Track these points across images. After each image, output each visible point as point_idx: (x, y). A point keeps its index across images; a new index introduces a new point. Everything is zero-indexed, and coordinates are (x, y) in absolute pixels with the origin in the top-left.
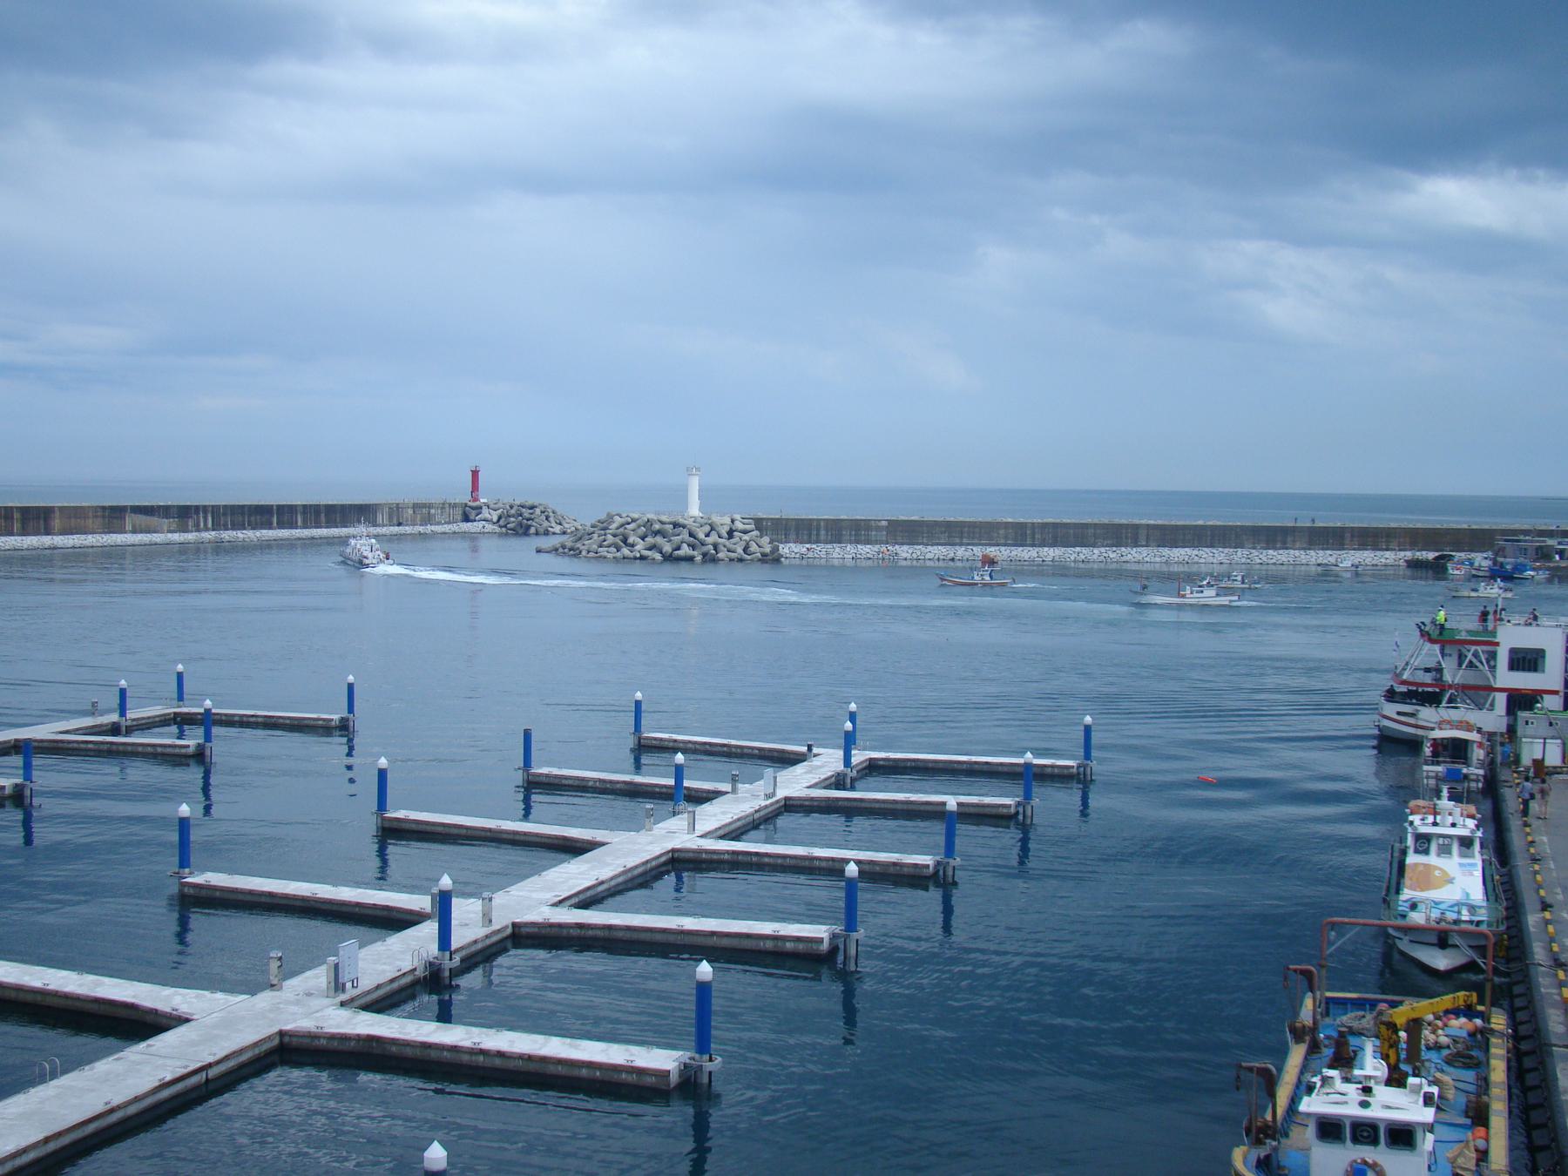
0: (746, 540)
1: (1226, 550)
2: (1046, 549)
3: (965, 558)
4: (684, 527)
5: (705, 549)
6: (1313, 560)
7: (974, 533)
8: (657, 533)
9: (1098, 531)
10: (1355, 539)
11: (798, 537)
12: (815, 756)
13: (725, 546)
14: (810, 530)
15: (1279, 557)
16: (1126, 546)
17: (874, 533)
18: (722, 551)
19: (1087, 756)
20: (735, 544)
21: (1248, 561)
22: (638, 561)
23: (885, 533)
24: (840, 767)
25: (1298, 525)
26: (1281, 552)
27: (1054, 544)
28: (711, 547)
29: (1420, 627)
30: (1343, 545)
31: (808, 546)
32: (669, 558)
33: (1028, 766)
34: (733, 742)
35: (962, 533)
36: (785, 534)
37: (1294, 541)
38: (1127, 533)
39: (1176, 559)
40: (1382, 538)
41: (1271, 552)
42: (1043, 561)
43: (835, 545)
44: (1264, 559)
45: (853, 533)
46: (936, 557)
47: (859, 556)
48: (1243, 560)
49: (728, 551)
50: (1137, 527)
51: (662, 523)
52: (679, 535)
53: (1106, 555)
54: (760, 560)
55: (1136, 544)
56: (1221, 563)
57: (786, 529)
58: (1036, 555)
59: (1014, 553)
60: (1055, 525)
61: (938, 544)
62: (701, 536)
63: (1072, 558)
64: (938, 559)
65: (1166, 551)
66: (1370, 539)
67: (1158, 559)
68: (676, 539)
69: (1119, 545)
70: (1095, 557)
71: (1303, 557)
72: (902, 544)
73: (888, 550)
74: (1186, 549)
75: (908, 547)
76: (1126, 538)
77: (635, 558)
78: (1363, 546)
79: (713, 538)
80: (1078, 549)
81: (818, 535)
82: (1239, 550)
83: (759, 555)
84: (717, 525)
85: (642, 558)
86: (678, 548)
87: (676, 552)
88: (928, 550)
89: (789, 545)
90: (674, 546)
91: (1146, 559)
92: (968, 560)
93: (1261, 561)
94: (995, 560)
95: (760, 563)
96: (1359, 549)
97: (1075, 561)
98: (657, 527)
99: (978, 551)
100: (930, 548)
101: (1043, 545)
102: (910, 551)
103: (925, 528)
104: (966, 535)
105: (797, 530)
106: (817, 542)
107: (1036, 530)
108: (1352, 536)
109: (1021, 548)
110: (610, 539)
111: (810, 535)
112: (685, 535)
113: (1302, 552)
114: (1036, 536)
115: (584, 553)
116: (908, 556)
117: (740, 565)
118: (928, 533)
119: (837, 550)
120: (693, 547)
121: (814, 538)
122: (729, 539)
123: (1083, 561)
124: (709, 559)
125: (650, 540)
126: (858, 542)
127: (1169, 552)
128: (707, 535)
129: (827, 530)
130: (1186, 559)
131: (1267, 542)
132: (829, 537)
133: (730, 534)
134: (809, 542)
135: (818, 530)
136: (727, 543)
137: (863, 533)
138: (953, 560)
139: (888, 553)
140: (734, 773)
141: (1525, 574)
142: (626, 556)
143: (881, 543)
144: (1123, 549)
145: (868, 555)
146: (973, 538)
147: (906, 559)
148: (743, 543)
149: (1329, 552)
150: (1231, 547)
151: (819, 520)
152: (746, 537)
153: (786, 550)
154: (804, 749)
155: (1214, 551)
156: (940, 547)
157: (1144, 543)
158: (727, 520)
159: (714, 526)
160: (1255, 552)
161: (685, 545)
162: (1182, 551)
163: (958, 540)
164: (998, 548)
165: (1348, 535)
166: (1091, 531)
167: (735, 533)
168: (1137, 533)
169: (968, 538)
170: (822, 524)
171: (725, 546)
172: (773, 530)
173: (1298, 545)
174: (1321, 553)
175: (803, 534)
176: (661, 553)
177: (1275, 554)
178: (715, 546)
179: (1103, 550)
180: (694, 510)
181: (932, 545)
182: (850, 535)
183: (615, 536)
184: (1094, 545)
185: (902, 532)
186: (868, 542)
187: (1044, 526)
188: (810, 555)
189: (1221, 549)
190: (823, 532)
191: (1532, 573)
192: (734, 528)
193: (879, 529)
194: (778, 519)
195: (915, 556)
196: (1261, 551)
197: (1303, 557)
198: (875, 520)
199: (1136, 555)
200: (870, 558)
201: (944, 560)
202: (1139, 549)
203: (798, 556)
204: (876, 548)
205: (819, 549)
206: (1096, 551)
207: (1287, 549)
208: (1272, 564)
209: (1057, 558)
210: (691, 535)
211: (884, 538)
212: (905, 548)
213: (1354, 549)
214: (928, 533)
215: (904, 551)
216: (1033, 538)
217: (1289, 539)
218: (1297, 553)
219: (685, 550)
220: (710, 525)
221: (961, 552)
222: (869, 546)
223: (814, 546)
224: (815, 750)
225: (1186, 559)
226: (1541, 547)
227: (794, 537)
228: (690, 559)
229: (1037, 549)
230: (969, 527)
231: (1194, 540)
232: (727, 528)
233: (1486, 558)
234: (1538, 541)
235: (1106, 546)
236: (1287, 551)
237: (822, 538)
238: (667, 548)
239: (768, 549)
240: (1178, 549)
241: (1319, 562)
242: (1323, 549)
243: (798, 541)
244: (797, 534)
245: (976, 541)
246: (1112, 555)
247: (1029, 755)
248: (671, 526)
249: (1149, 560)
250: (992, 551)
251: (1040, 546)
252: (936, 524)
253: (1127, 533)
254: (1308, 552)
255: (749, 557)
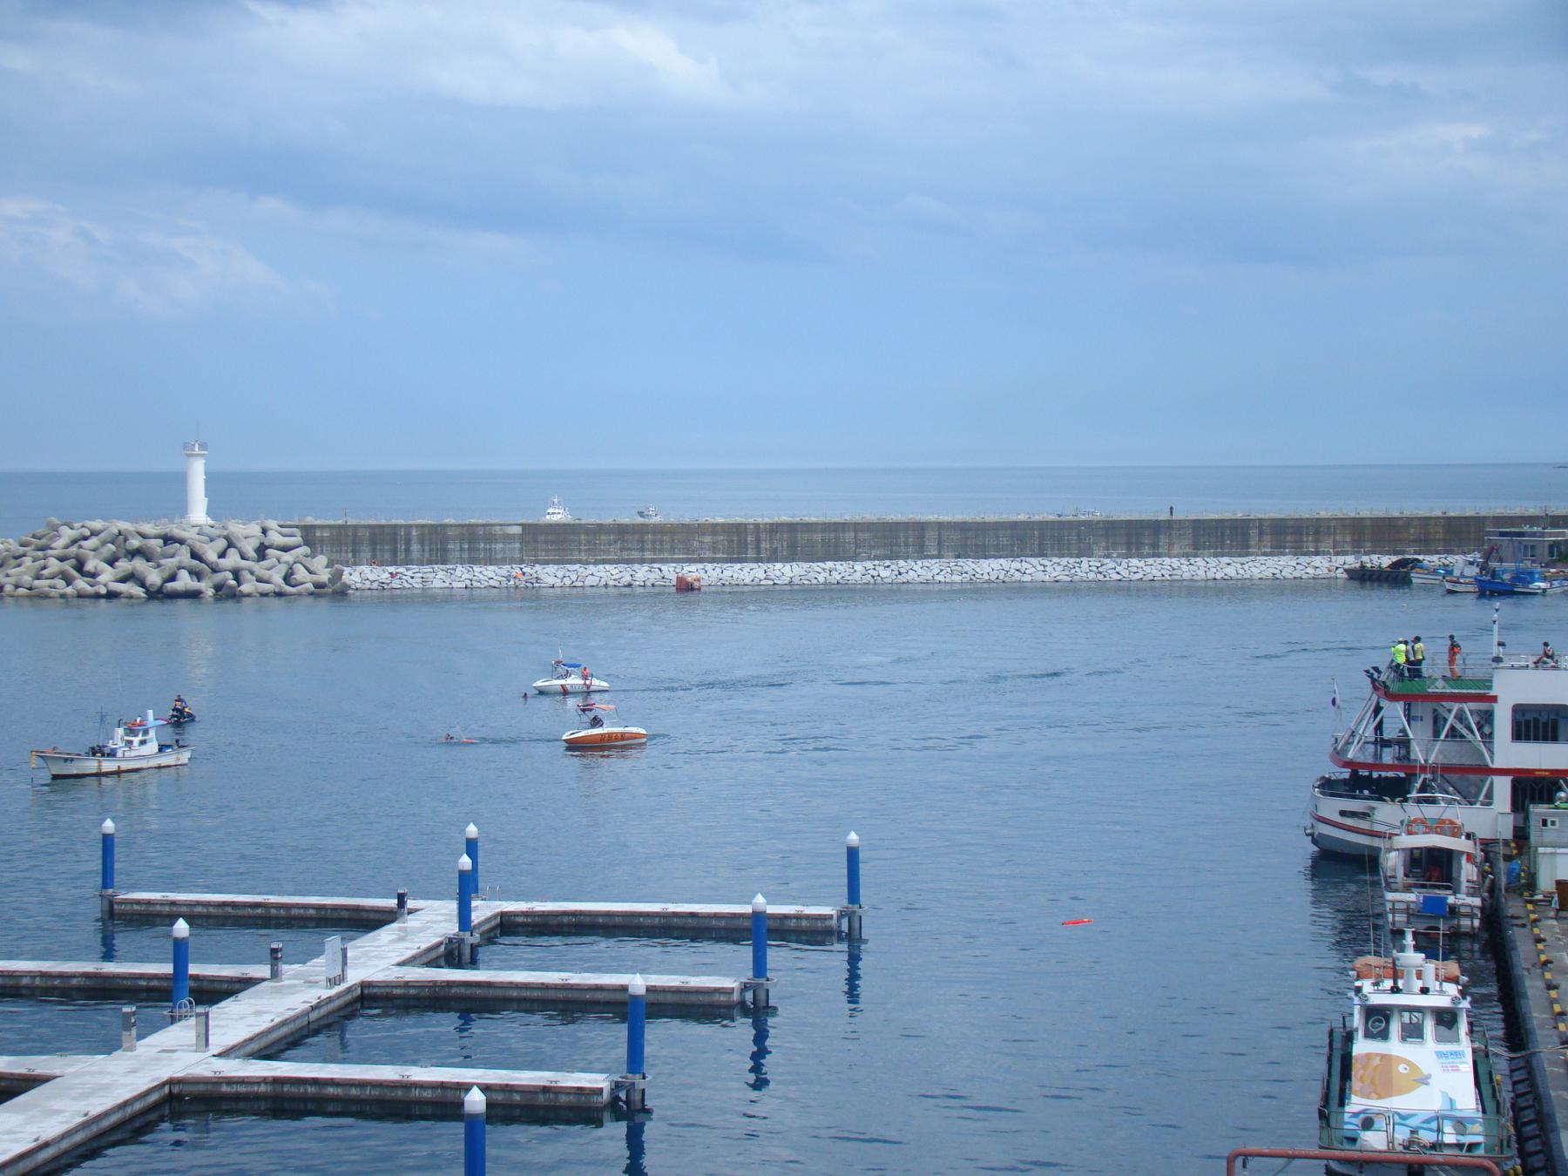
0: (286, 562)
1: (1064, 561)
2: (779, 565)
3: (649, 583)
4: (181, 542)
5: (218, 577)
6: (1201, 573)
7: (661, 542)
8: (133, 554)
9: (861, 535)
10: (1265, 538)
11: (374, 556)
12: (411, 912)
13: (252, 573)
14: (394, 542)
15: (1148, 569)
16: (906, 558)
17: (500, 546)
18: (250, 581)
19: (853, 894)
20: (269, 570)
21: (1100, 577)
22: (103, 601)
23: (517, 545)
24: (453, 928)
25: (1174, 518)
26: (1150, 561)
27: (791, 558)
28: (230, 575)
29: (1371, 676)
30: (1248, 547)
31: (392, 569)
32: (158, 595)
33: (758, 916)
34: (273, 899)
35: (643, 542)
36: (354, 552)
37: (1170, 545)
38: (907, 537)
39: (986, 577)
40: (1308, 534)
41: (1134, 561)
42: (774, 584)
43: (436, 566)
44: (1125, 573)
45: (466, 546)
46: (603, 582)
47: (475, 584)
48: (1091, 576)
49: (260, 580)
50: (922, 527)
51: (144, 536)
52: (173, 556)
53: (875, 573)
54: (312, 594)
55: (921, 554)
56: (1057, 581)
57: (354, 543)
58: (764, 575)
59: (727, 573)
60: (792, 527)
61: (604, 562)
62: (212, 556)
63: (821, 579)
64: (606, 586)
65: (969, 565)
66: (1289, 538)
67: (957, 578)
68: (169, 563)
69: (893, 556)
70: (857, 576)
71: (1184, 568)
72: (547, 562)
73: (524, 574)
74: (1002, 561)
75: (556, 567)
76: (907, 545)
77: (97, 596)
78: (1278, 549)
79: (233, 559)
80: (830, 564)
81: (407, 550)
82: (1085, 560)
83: (310, 586)
84: (238, 539)
85: (111, 595)
86: (173, 578)
87: (170, 585)
88: (588, 572)
89: (359, 568)
90: (166, 575)
91: (937, 578)
92: (653, 585)
93: (1119, 577)
94: (696, 584)
95: (311, 599)
96: (1272, 554)
97: (825, 583)
98: (135, 543)
99: (671, 572)
100: (592, 568)
101: (773, 557)
102: (560, 574)
103: (583, 537)
104: (650, 546)
105: (373, 542)
106: (407, 562)
107: (763, 536)
108: (1261, 533)
109: (738, 566)
110: (54, 565)
111: (394, 552)
112: (184, 556)
113: (1183, 560)
114: (763, 545)
115: (8, 588)
116: (558, 582)
117: (276, 601)
118: (589, 542)
119: (441, 575)
120: (197, 574)
121: (401, 556)
122: (258, 561)
123: (838, 583)
124: (226, 594)
125: (124, 565)
126: (473, 561)
127: (973, 566)
128: (222, 555)
129: (422, 542)
130: (1002, 576)
131: (1129, 545)
132: (427, 555)
133: (261, 552)
134: (394, 563)
135: (408, 542)
136: (259, 568)
137: (482, 545)
138: (630, 585)
139: (524, 578)
140: (274, 946)
141: (1531, 586)
142: (82, 592)
143: (512, 561)
144: (902, 563)
145: (492, 583)
146: (661, 551)
147: (553, 587)
148: (283, 569)
149: (1226, 560)
150: (1071, 557)
151: (409, 527)
152: (288, 557)
153: (356, 578)
154: (392, 903)
155: (1045, 562)
156: (608, 567)
157: (935, 553)
158: (256, 530)
159: (233, 539)
160: (1109, 563)
161: (184, 574)
162: (995, 564)
163: (636, 555)
164: (700, 566)
165: (1254, 533)
166: (849, 536)
167: (269, 551)
168: (922, 537)
169: (654, 550)
170: (414, 533)
171: (252, 573)
172: (332, 545)
173: (1176, 550)
174: (1213, 561)
175: (382, 551)
176: (143, 585)
177: (1141, 564)
178: (236, 574)
179: (869, 564)
180: (199, 513)
181: (596, 563)
182: (462, 550)
183: (62, 559)
184: (855, 558)
185: (546, 542)
186: (490, 561)
187: (775, 528)
188: (396, 584)
189: (1055, 560)
190: (415, 547)
191: (1543, 585)
192: (267, 543)
193: (508, 538)
194: (340, 526)
195: (567, 582)
196: (1119, 560)
197: (1184, 568)
198: (501, 525)
199: (920, 572)
200: (495, 587)
201: (615, 586)
202: (926, 563)
203: (375, 585)
204: (504, 570)
205: (410, 573)
206: (858, 567)
207: (1159, 555)
208: (1138, 580)
209: (796, 581)
210: (195, 555)
211: (517, 555)
212: (551, 569)
213: (1265, 554)
214: (589, 542)
215: (551, 575)
216: (758, 548)
217: (1163, 540)
218: (1175, 562)
219: (184, 582)
220: (227, 538)
221: (642, 573)
222: (491, 568)
223: (401, 569)
224: (410, 904)
225: (1002, 576)
226: (1557, 543)
227: (369, 555)
228: (194, 595)
229: (764, 566)
230: (654, 533)
231: (1012, 546)
232: (255, 543)
233: (1471, 563)
234: (1551, 535)
235: (874, 560)
236: (1159, 560)
237: (415, 555)
238: (154, 578)
239: (324, 576)
240: (987, 561)
241: (1210, 575)
242: (1215, 555)
243: (373, 562)
244: (374, 551)
245: (666, 556)
246: (885, 573)
247: (760, 900)
248: (161, 542)
249: (943, 580)
250: (691, 571)
251: (769, 561)
252: (600, 529)
253: (907, 537)
254: (1192, 561)
255: (293, 590)
